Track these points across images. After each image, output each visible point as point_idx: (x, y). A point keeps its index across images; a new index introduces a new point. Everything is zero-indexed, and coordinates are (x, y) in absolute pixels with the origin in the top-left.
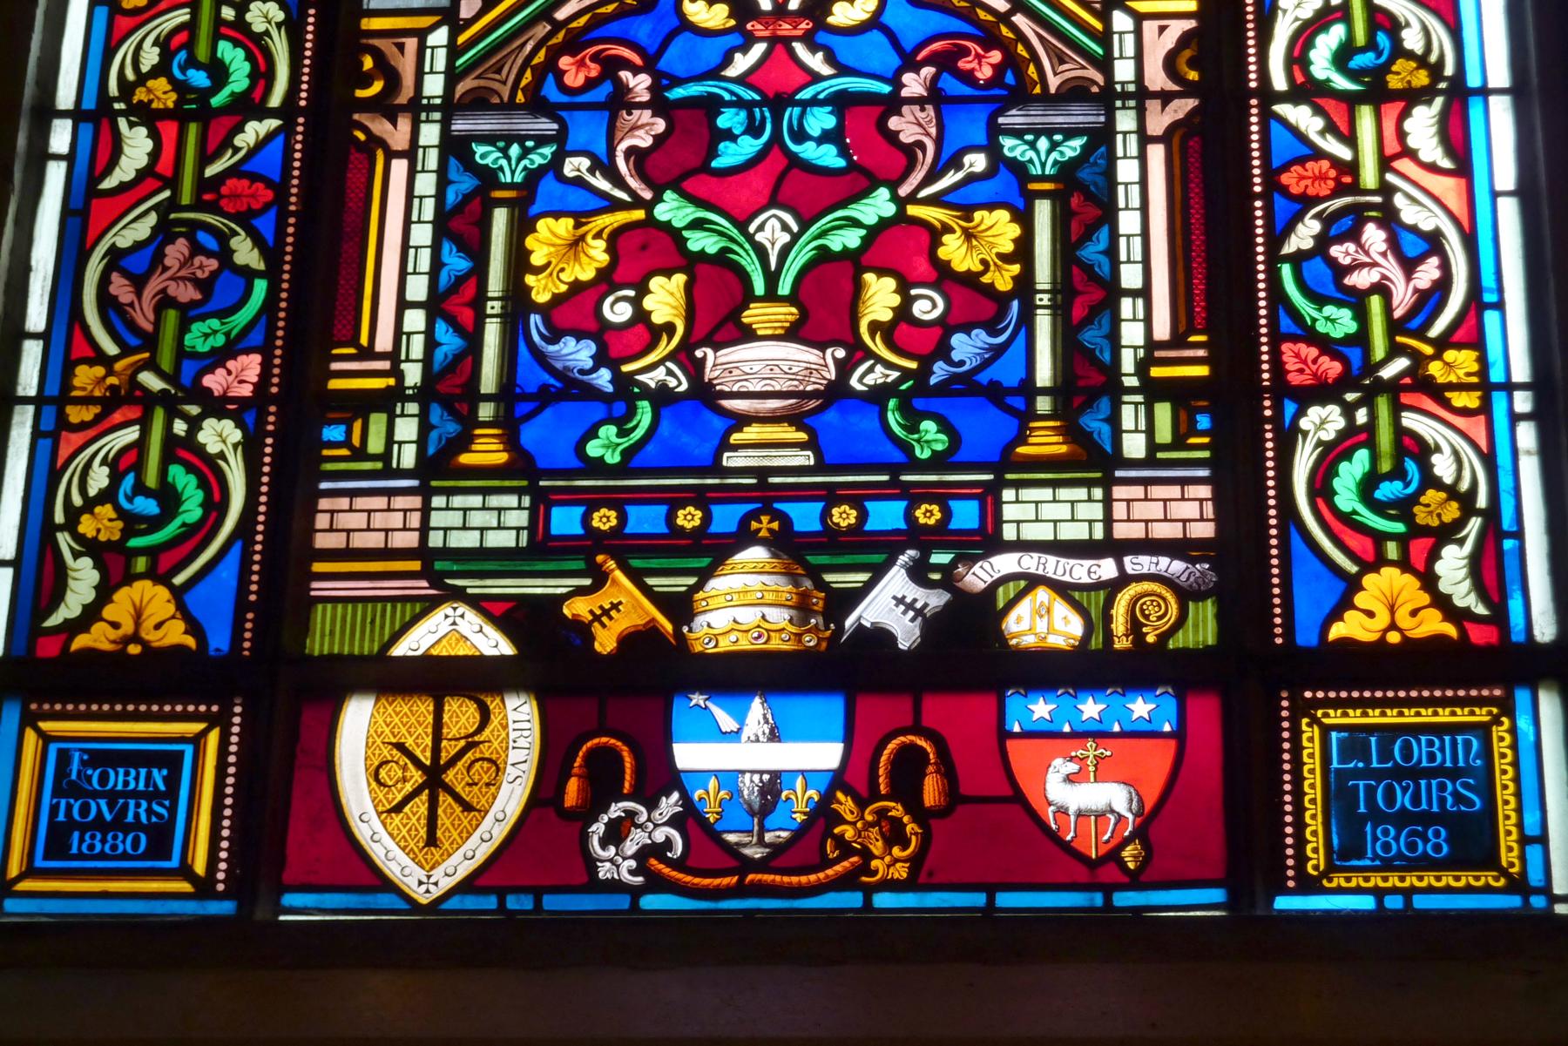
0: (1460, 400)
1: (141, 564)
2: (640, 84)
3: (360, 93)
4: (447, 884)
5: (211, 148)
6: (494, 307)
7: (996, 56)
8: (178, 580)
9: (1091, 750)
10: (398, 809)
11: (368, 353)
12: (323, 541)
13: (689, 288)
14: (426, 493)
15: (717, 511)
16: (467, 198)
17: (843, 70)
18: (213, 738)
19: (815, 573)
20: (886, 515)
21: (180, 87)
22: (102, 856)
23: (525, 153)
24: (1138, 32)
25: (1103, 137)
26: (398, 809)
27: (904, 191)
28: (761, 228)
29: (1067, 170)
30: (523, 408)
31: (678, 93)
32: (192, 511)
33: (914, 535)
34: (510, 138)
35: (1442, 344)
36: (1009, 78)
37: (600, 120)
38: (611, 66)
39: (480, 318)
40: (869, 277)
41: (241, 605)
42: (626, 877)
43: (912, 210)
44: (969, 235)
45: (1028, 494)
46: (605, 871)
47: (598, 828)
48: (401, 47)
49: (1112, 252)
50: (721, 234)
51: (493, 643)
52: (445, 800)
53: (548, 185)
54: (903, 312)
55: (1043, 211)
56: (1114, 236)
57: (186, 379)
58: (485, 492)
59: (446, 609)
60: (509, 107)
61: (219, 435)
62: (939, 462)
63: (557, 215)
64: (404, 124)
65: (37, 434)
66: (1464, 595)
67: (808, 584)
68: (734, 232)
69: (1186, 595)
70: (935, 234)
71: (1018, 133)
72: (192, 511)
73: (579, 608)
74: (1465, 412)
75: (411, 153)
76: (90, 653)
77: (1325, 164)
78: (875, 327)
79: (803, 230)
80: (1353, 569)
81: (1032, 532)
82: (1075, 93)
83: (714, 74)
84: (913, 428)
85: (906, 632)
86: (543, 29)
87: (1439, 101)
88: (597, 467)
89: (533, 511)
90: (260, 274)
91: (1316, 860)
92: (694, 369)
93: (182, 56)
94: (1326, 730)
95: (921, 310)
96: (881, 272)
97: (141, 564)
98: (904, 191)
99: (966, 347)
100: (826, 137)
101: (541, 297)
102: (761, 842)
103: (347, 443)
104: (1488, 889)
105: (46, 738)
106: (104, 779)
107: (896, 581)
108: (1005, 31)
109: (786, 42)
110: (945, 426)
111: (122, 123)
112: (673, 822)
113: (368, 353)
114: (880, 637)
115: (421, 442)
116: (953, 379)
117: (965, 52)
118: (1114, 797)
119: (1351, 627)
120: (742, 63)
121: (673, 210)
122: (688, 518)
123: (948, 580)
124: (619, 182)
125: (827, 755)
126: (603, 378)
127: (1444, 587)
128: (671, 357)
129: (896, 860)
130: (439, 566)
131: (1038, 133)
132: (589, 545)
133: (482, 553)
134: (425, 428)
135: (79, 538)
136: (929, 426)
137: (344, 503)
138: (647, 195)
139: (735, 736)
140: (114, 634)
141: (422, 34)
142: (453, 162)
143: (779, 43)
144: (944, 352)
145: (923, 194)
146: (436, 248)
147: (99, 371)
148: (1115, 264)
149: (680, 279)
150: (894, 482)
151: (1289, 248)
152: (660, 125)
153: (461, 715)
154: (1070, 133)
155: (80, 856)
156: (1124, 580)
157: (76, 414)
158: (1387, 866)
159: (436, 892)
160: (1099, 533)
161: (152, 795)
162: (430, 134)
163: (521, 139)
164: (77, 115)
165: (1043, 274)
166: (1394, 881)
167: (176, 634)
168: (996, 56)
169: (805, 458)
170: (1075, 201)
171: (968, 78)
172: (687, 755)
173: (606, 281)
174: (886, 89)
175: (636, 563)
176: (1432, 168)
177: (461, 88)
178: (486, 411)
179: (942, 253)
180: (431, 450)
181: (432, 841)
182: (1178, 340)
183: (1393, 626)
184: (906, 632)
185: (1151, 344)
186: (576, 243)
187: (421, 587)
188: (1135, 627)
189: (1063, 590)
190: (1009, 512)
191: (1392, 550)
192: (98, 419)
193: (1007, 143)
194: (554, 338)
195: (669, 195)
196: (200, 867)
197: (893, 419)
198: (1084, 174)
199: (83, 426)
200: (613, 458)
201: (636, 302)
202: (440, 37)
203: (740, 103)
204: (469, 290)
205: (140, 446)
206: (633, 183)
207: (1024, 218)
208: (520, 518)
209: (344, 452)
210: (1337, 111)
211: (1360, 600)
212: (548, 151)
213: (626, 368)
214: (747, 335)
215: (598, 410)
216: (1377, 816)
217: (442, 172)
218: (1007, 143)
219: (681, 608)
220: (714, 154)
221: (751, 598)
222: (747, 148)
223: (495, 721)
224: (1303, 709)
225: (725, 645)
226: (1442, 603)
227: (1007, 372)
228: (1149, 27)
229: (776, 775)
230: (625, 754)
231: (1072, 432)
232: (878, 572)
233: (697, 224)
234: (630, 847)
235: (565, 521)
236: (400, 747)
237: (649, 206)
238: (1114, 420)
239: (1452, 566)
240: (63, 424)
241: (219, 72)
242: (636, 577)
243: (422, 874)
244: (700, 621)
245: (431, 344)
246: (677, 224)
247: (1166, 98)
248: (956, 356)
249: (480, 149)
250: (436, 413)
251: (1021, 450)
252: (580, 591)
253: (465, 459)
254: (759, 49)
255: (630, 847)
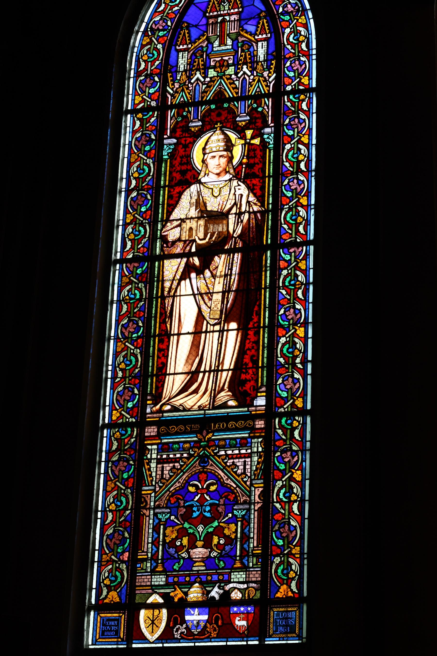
0: (297, 556)
1: (113, 588)
2: (182, 502)
3: (142, 505)
4: (155, 639)
5: (121, 516)
6: (161, 543)
7: (234, 496)
8: (118, 591)
9: (242, 616)
10: (148, 627)
11: (143, 552)
12: (137, 584)
13: (188, 539)
14: (151, 575)
15: (192, 577)
16: (157, 524)
17: (211, 499)
18: (123, 616)
19: (205, 587)
20: (215, 578)
21: (116, 505)
22: (109, 635)
23: (165, 515)
24: (255, 491)
25: (249, 510)
26: (148, 627)
27: (219, 521)
28: (199, 528)
29: (243, 516)
30: (164, 561)
31: (187, 504)
32: (119, 580)
33: (220, 581)
34: (163, 513)
35: (295, 546)
36: (235, 500)
37: (175, 509)
38: (178, 499)
39: (159, 545)
40: (214, 536)
41: (127, 595)
42: (179, 637)
43: (221, 524)
44: (229, 528)
45: (235, 573)
46: (176, 636)
47: (175, 629)
48: (147, 497)
49: (249, 531)
50: (193, 529)
51: (161, 601)
52: (154, 625)
53: (168, 520)
54: (219, 542)
55: (239, 523)
56: (250, 528)
57: (118, 557)
58: (160, 575)
59: (154, 595)
60: (163, 507)
61: (124, 567)
62: (223, 568)
63: (170, 527)
64: (148, 511)
65: (98, 567)
66: (295, 590)
67: (204, 589)
68: (195, 529)
69: (256, 590)
70: (223, 528)
71: (236, 510)
72: (119, 580)
73: (172, 594)
74: (297, 558)
75: (149, 516)
76: (106, 603)
77: (281, 514)
78: (215, 545)
79: (205, 528)
80: (280, 585)
81: (236, 580)
82: (245, 502)
83: (193, 500)
84: (219, 563)
85: (217, 597)
86: (168, 492)
87: (298, 502)
88: (175, 571)
89: (166, 578)
90: (128, 538)
91: (271, 632)
92: (189, 553)
93: (116, 500)
94: (274, 612)
95: (222, 542)
96: (216, 536)
97: (113, 588)
98: (219, 521)
99: (227, 548)
100: (209, 511)
101: (167, 541)
102: (197, 631)
103: (140, 567)
104: (294, 637)
105: (101, 617)
106: (109, 623)
107: (216, 589)
108: (235, 491)
109: (203, 494)
110: (224, 563)
111: (108, 512)
112: (185, 628)
113: (143, 552)
114: (213, 598)
115: (151, 567)
116: (225, 554)
117: (229, 495)
118: (244, 623)
119: (279, 595)
120: (197, 498)
121: (186, 525)
122: (187, 579)
123: (223, 589)
124: (179, 520)
125: (206, 617)
126: (176, 555)
127: (292, 588)
128: (186, 551)
129: (215, 634)
130: (153, 588)
131: (239, 510)
132: (174, 583)
133: (159, 585)
134: (151, 564)
135: (104, 584)
136: (221, 562)
137: (140, 577)
138: (183, 522)
139: (193, 614)
140: (110, 600)
141: (150, 494)
142: (155, 517)
143: (202, 495)
144: (224, 549)
145: (223, 521)
146: (153, 533)
147: (106, 556)
148: (250, 533)
149: (187, 537)
150: (216, 572)
151: (274, 529)
152: (185, 510)
153: (156, 612)
154: (244, 510)
155: (106, 636)
156: (248, 587)
157: (103, 563)
158: (281, 633)
159: (153, 640)
160: (244, 580)
161: (115, 626)
162: (152, 512)
163: (165, 513)
164: (101, 511)
165: (239, 535)
166: (281, 636)
167: (118, 600)
168: (234, 496)
169: (203, 568)
170: (244, 522)
171: (229, 500)
172: (187, 618)
173: (177, 538)
174: (218, 502)
175: (180, 587)
176: (296, 514)
177: (157, 503)
178: (160, 561)
179: (225, 532)
180: (152, 568)
181: (153, 632)
182: (257, 546)
183: (284, 595)
184: (217, 597)
185: (254, 547)
186: (172, 531)
187: (150, 591)
188: (249, 595)
189: (239, 589)
190: (232, 577)
191: (285, 581)
192: (106, 564)
193: (235, 511)
194: (169, 549)
195: (186, 523)
196: (122, 637)
197: (217, 561)
198: (246, 517)
199: (104, 565)
200: (177, 569)
201: (181, 542)
202: (153, 495)
203: (197, 506)
204: (158, 540)
205: (112, 568)
206: (180, 520)
207: (237, 525)
208: (164, 579)
209: (140, 569)
210: (283, 504)
211: (281, 590)
212: (169, 515)
213: (179, 553)
214: (196, 547)
215: (176, 561)
216: (280, 625)
217: (153, 519)
218: (235, 511)
219: (186, 594)
220: (192, 515)
221: (196, 592)
222: (198, 513)
223: (161, 613)
224: (271, 608)
225: (192, 600)
226: (291, 590)
227: (232, 554)
228: (256, 490)
229: (199, 620)
230: (179, 618)
231: (242, 563)
232: (214, 587)
233: (190, 528)
234: (179, 632)
235: (170, 580)
236: (148, 617)
237: (183, 524)
238: (248, 560)
239: (293, 585)
240: (101, 565)
241: (122, 502)
242: (180, 589)
243: (151, 637)
244: (189, 597)
245: (152, 550)
246: (187, 528)
247: (258, 503)
248: (226, 550)
249: (159, 515)
250: (153, 562)
251: (235, 566)
252: (173, 591)
253: (157, 569)
254: (199, 495)
255: (179, 632)
